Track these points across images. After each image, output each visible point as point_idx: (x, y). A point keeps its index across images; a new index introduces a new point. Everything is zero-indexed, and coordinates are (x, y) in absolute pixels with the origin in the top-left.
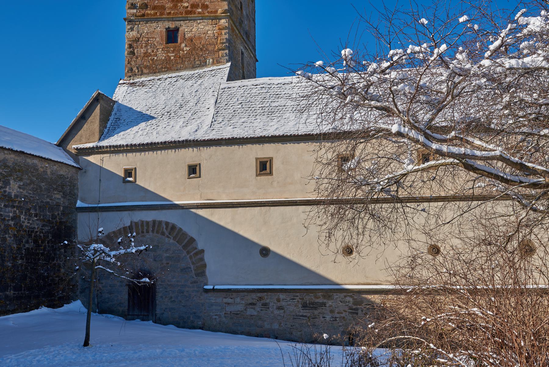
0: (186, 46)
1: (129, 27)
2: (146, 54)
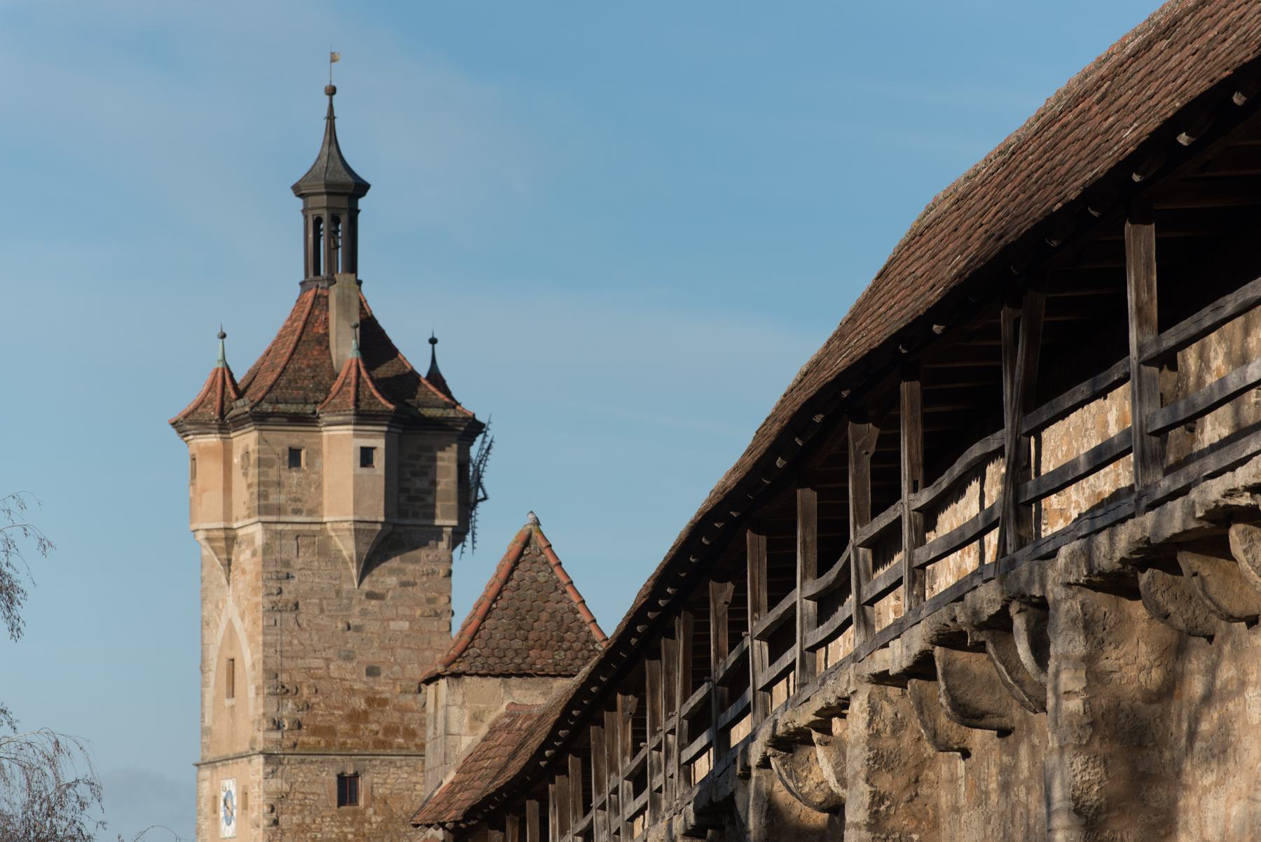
0: (375, 813)
1: (269, 770)
2: (302, 828)
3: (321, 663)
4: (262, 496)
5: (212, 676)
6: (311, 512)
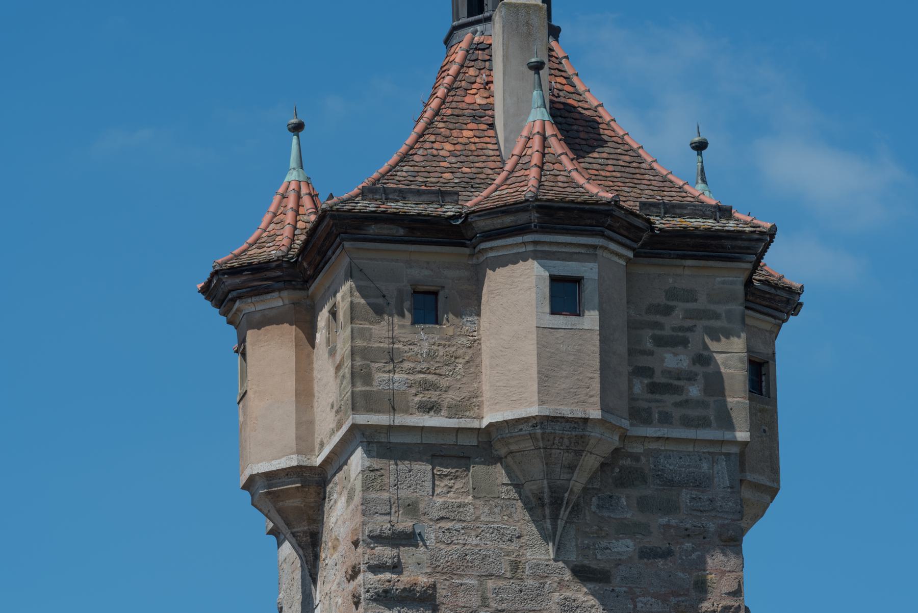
4: (359, 375)
6: (456, 410)
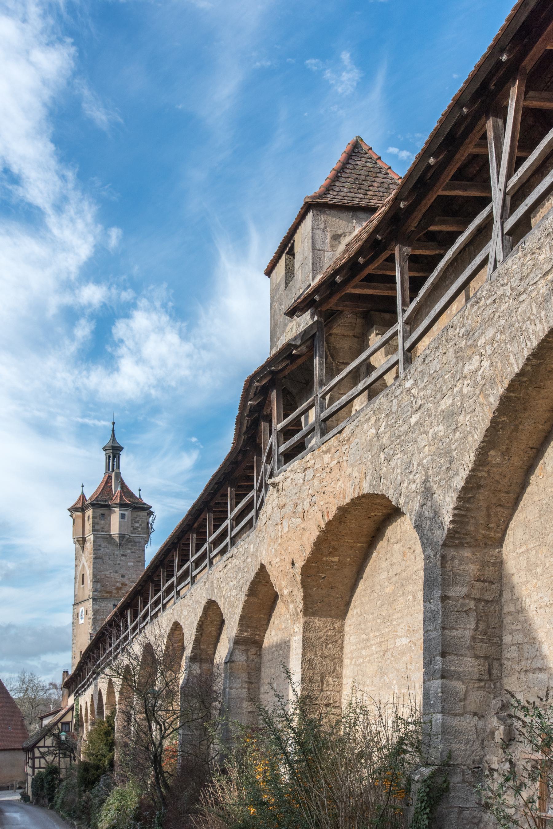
3: (109, 573)
4: (93, 527)
5: (78, 580)
6: (106, 532)
